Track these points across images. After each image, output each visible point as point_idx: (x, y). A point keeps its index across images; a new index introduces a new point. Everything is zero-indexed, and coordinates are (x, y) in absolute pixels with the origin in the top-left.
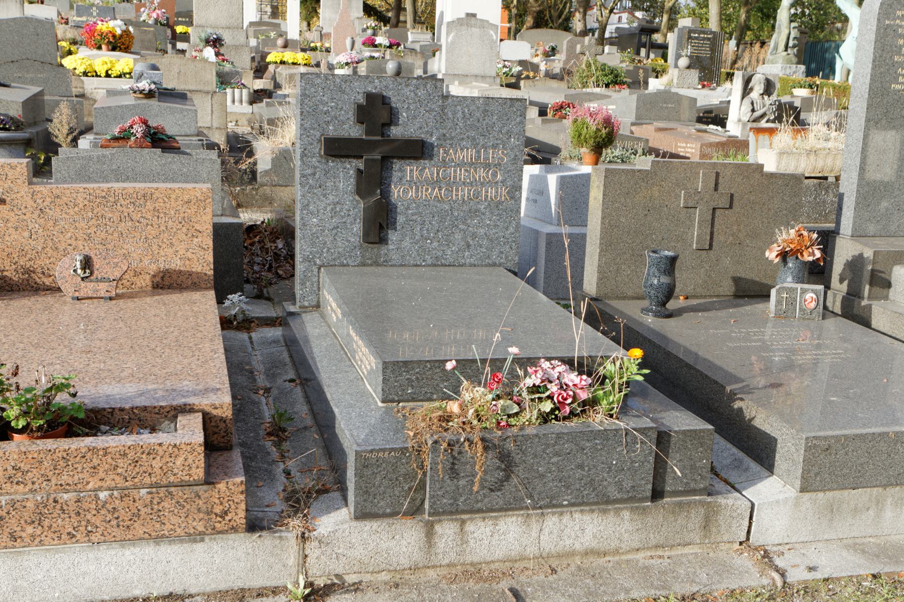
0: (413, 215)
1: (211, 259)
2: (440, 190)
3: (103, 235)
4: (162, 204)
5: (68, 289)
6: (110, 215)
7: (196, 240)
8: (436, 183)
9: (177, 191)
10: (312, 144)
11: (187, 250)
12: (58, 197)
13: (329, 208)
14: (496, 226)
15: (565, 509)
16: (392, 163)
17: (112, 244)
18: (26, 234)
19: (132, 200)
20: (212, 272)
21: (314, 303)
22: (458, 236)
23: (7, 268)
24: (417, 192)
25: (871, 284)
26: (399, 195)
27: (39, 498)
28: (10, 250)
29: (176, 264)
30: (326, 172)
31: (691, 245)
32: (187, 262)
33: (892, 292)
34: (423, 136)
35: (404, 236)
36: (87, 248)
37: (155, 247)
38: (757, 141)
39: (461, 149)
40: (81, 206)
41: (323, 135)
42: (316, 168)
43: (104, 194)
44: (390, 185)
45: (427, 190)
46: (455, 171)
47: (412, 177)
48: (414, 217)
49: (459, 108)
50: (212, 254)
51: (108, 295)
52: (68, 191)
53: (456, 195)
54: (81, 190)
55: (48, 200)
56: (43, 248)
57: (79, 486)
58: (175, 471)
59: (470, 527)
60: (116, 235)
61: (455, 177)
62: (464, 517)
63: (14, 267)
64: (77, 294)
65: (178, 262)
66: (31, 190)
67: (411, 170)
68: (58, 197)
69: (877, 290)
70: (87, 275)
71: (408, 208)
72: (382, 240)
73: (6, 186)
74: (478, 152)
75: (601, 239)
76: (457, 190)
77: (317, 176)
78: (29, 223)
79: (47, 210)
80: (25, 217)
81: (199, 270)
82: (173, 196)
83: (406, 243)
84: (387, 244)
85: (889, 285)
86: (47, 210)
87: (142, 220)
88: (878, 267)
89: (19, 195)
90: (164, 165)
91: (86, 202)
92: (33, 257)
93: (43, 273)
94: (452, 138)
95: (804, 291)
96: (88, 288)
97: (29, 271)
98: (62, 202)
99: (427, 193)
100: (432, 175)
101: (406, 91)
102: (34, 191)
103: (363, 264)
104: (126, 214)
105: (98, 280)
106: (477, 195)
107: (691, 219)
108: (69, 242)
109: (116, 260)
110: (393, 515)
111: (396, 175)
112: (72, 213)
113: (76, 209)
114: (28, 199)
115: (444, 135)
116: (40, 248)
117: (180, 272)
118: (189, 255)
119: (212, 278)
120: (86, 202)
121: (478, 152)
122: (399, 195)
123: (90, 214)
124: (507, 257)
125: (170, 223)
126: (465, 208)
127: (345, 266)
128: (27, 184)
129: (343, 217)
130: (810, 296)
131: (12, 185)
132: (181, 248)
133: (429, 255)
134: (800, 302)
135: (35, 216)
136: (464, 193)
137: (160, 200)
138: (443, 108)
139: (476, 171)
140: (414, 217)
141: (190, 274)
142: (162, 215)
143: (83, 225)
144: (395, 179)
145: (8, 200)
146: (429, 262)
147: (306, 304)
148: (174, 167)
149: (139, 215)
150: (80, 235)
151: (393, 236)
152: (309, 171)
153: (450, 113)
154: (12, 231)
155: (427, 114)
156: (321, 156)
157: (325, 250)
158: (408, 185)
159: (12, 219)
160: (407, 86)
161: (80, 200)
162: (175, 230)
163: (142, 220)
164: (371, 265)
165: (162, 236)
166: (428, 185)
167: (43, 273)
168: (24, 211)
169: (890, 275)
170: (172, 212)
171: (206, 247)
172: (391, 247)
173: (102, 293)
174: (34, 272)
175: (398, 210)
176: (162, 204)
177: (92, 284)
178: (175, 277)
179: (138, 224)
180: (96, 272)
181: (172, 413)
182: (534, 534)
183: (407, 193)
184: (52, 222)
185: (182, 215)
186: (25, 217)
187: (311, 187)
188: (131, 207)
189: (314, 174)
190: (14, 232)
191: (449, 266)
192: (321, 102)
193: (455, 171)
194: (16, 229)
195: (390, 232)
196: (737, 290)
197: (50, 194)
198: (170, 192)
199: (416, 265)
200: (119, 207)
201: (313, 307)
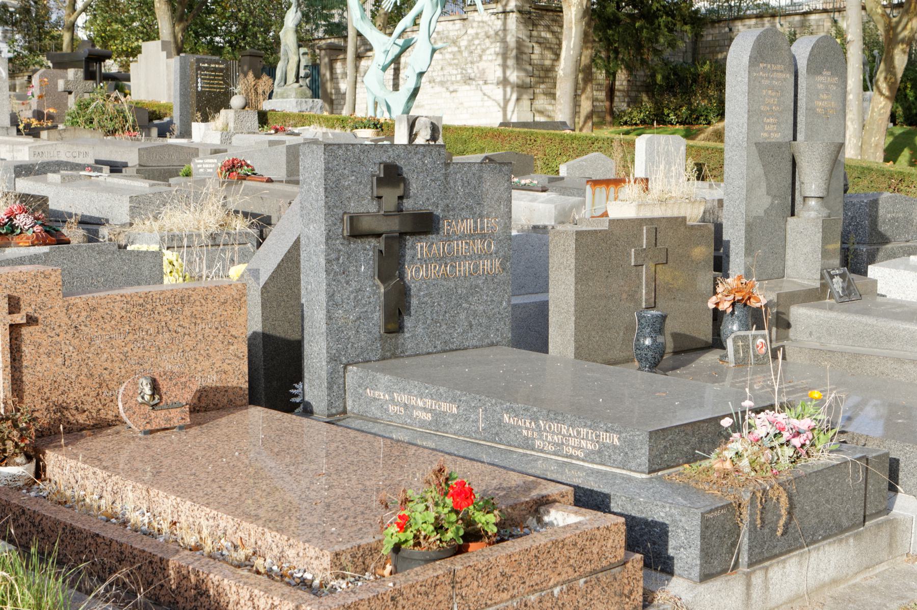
0: (424, 296)
1: (246, 370)
2: (446, 266)
3: (140, 353)
4: (199, 308)
5: (135, 424)
6: (148, 327)
7: (232, 348)
8: (441, 260)
9: (214, 290)
10: (335, 224)
11: (223, 361)
12: (94, 309)
13: (352, 297)
14: (492, 301)
15: (820, 544)
16: (405, 240)
17: (149, 362)
18: (59, 360)
19: (170, 306)
20: (246, 386)
21: (341, 409)
22: (463, 316)
23: (38, 407)
24: (427, 270)
25: (777, 327)
26: (412, 276)
27: (515, 604)
28: (42, 383)
29: (213, 380)
30: (349, 256)
31: (640, 305)
32: (224, 376)
33: (791, 332)
34: (430, 208)
35: (418, 321)
36: (123, 371)
37: (192, 361)
38: (594, 194)
39: (462, 220)
40: (118, 318)
41: (345, 213)
42: (340, 251)
43: (141, 301)
44: (404, 265)
45: (435, 267)
46: (458, 245)
47: (422, 254)
48: (425, 299)
49: (459, 175)
50: (246, 363)
51: (182, 423)
52: (105, 301)
53: (460, 271)
54: (118, 298)
55: (84, 314)
56: (77, 376)
57: (544, 584)
58: (607, 554)
59: (771, 574)
60: (153, 350)
61: (458, 252)
62: (767, 564)
63: (45, 404)
64: (148, 427)
65: (215, 378)
66: (66, 303)
67: (422, 247)
68: (94, 309)
69: (781, 330)
70: (156, 401)
71: (419, 290)
72: (400, 329)
73: (39, 300)
74: (475, 222)
75: (576, 305)
76: (460, 266)
77: (341, 261)
78: (63, 345)
79: (83, 328)
80: (58, 339)
81: (235, 384)
82: (210, 297)
83: (420, 330)
84: (403, 332)
85: (788, 326)
86: (83, 328)
87: (179, 329)
88: (781, 310)
89: (53, 311)
90: (104, 263)
91: (123, 313)
92: (66, 389)
93: (77, 409)
94: (454, 209)
95: (755, 337)
96: (159, 418)
97: (61, 408)
98: (98, 316)
99: (435, 270)
100: (439, 250)
101: (415, 160)
102: (69, 304)
103: (383, 358)
104: (163, 324)
105: (169, 407)
106: (477, 267)
107: (639, 277)
108: (105, 365)
109: (183, 380)
110: (724, 571)
111: (409, 253)
112: (109, 328)
113: (113, 322)
114: (62, 315)
115: (448, 206)
116: (73, 377)
117: (217, 388)
118: (225, 367)
119: (247, 392)
120: (123, 313)
121: (475, 222)
122: (412, 276)
123: (127, 327)
124: (502, 334)
125: (207, 330)
126: (467, 284)
127: (367, 362)
128: (61, 296)
129: (364, 306)
130: (760, 341)
131: (45, 299)
132: (217, 358)
133: (438, 340)
134: (753, 349)
135: (69, 336)
136: (465, 267)
137: (198, 303)
138: (446, 176)
139: (474, 243)
140: (425, 299)
141: (226, 390)
142: (199, 321)
143: (119, 342)
144: (408, 258)
145: (41, 318)
146: (439, 348)
147: (334, 411)
148: (114, 265)
149: (177, 324)
150: (117, 355)
151: (408, 322)
152: (333, 256)
153: (452, 182)
154: (44, 358)
155: (433, 184)
156: (344, 238)
157: (349, 346)
158: (422, 264)
159: (44, 343)
160: (416, 153)
161: (117, 312)
162: (211, 337)
163: (179, 329)
164: (390, 358)
165: (199, 347)
166: (436, 261)
167: (77, 409)
168: (58, 331)
169: (788, 316)
170: (209, 317)
171: (241, 355)
172: (407, 335)
173: (176, 422)
174: (67, 409)
175: (412, 293)
176: (199, 308)
177: (163, 413)
178: (211, 395)
179: (175, 335)
180: (164, 397)
181: (534, 507)
182: (804, 572)
183: (419, 272)
184: (87, 342)
185: (218, 319)
186: (58, 339)
187: (336, 274)
188: (168, 314)
189: (338, 259)
190: (46, 360)
191: (456, 350)
192: (342, 175)
193: (458, 245)
194: (49, 355)
195: (405, 318)
196: (675, 347)
197: (86, 307)
198: (207, 292)
199: (429, 353)
200: (156, 316)
201: (340, 414)
